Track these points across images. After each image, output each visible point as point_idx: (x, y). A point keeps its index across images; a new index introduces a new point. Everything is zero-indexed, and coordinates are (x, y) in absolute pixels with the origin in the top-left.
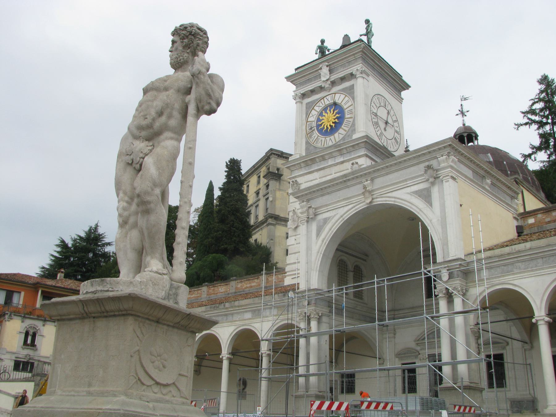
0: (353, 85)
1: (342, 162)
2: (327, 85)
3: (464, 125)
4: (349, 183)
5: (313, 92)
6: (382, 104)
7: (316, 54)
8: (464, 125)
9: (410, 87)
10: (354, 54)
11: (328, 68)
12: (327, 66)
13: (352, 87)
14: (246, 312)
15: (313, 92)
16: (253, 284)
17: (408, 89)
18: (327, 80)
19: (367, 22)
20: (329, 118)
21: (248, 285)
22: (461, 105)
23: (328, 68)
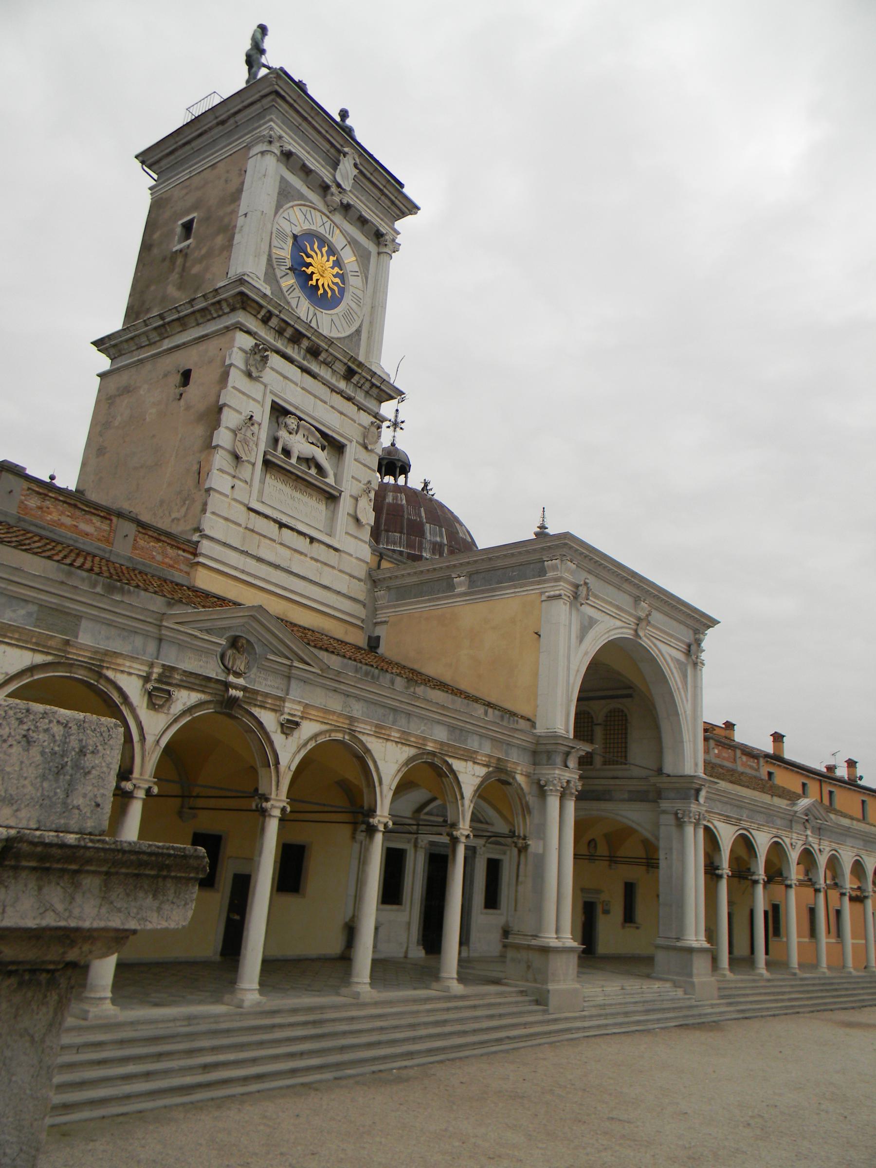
3: (393, 445)
4: (625, 586)
5: (306, 171)
8: (393, 445)
12: (356, 165)
14: (438, 722)
15: (306, 171)
16: (83, 526)
21: (68, 521)
22: (397, 410)
23: (356, 172)
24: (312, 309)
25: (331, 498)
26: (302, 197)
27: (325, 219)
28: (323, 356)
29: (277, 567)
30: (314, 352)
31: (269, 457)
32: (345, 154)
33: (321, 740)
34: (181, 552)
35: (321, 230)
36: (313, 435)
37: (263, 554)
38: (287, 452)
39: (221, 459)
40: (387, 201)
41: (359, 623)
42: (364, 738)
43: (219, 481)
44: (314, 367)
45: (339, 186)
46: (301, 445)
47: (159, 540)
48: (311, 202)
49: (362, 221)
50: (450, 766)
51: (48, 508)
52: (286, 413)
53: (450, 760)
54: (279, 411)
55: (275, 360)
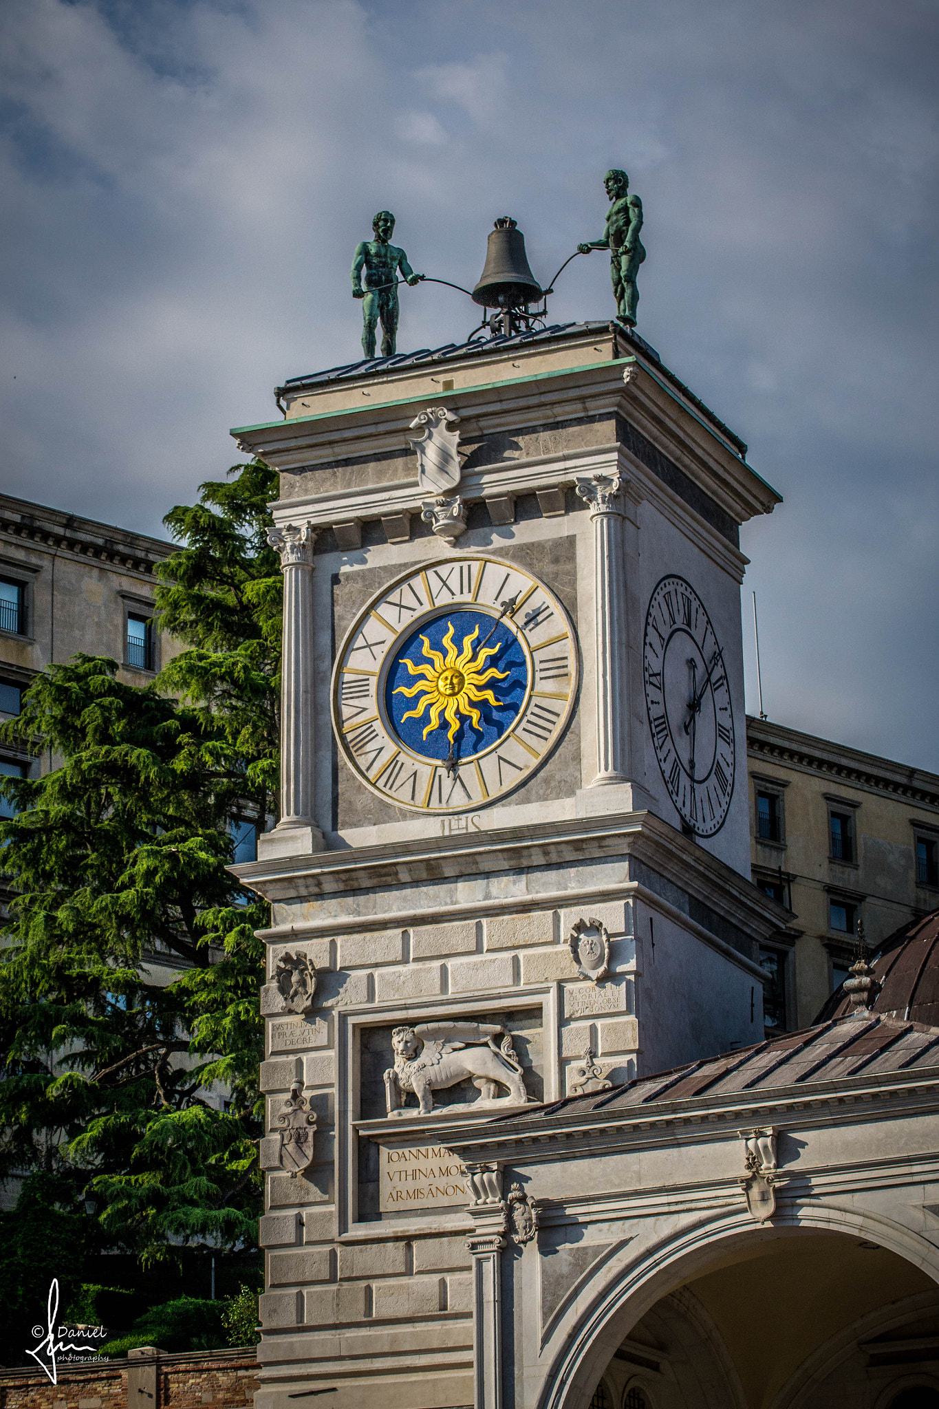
0: (571, 540)
1: (525, 908)
6: (680, 621)
7: (358, 294)
9: (779, 499)
10: (582, 399)
12: (451, 426)
13: (566, 549)
17: (768, 510)
19: (618, 183)
31: (362, 1133)
34: (241, 1373)
35: (444, 599)
40: (568, 408)
47: (202, 1371)
48: (406, 565)
51: (33, 1401)
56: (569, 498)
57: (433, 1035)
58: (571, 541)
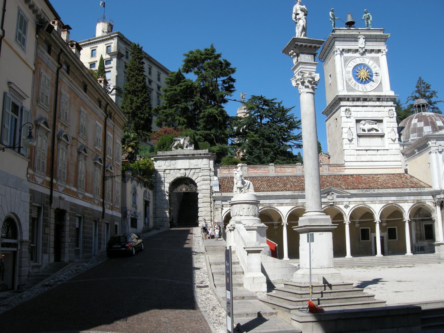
2: (361, 51)
5: (349, 51)
11: (364, 40)
12: (364, 38)
13: (378, 58)
18: (363, 48)
20: (363, 74)
24: (363, 87)
25: (382, 136)
26: (351, 57)
27: (360, 58)
28: (368, 100)
29: (368, 161)
30: (365, 100)
32: (359, 38)
33: (356, 207)
35: (360, 62)
36: (371, 122)
37: (362, 160)
38: (364, 130)
39: (346, 141)
41: (400, 167)
42: (368, 205)
43: (345, 147)
44: (366, 103)
45: (361, 48)
46: (367, 126)
49: (372, 51)
50: (399, 206)
52: (361, 120)
53: (398, 204)
54: (358, 121)
55: (352, 109)
56: (379, 51)
57: (367, 122)
58: (379, 57)
